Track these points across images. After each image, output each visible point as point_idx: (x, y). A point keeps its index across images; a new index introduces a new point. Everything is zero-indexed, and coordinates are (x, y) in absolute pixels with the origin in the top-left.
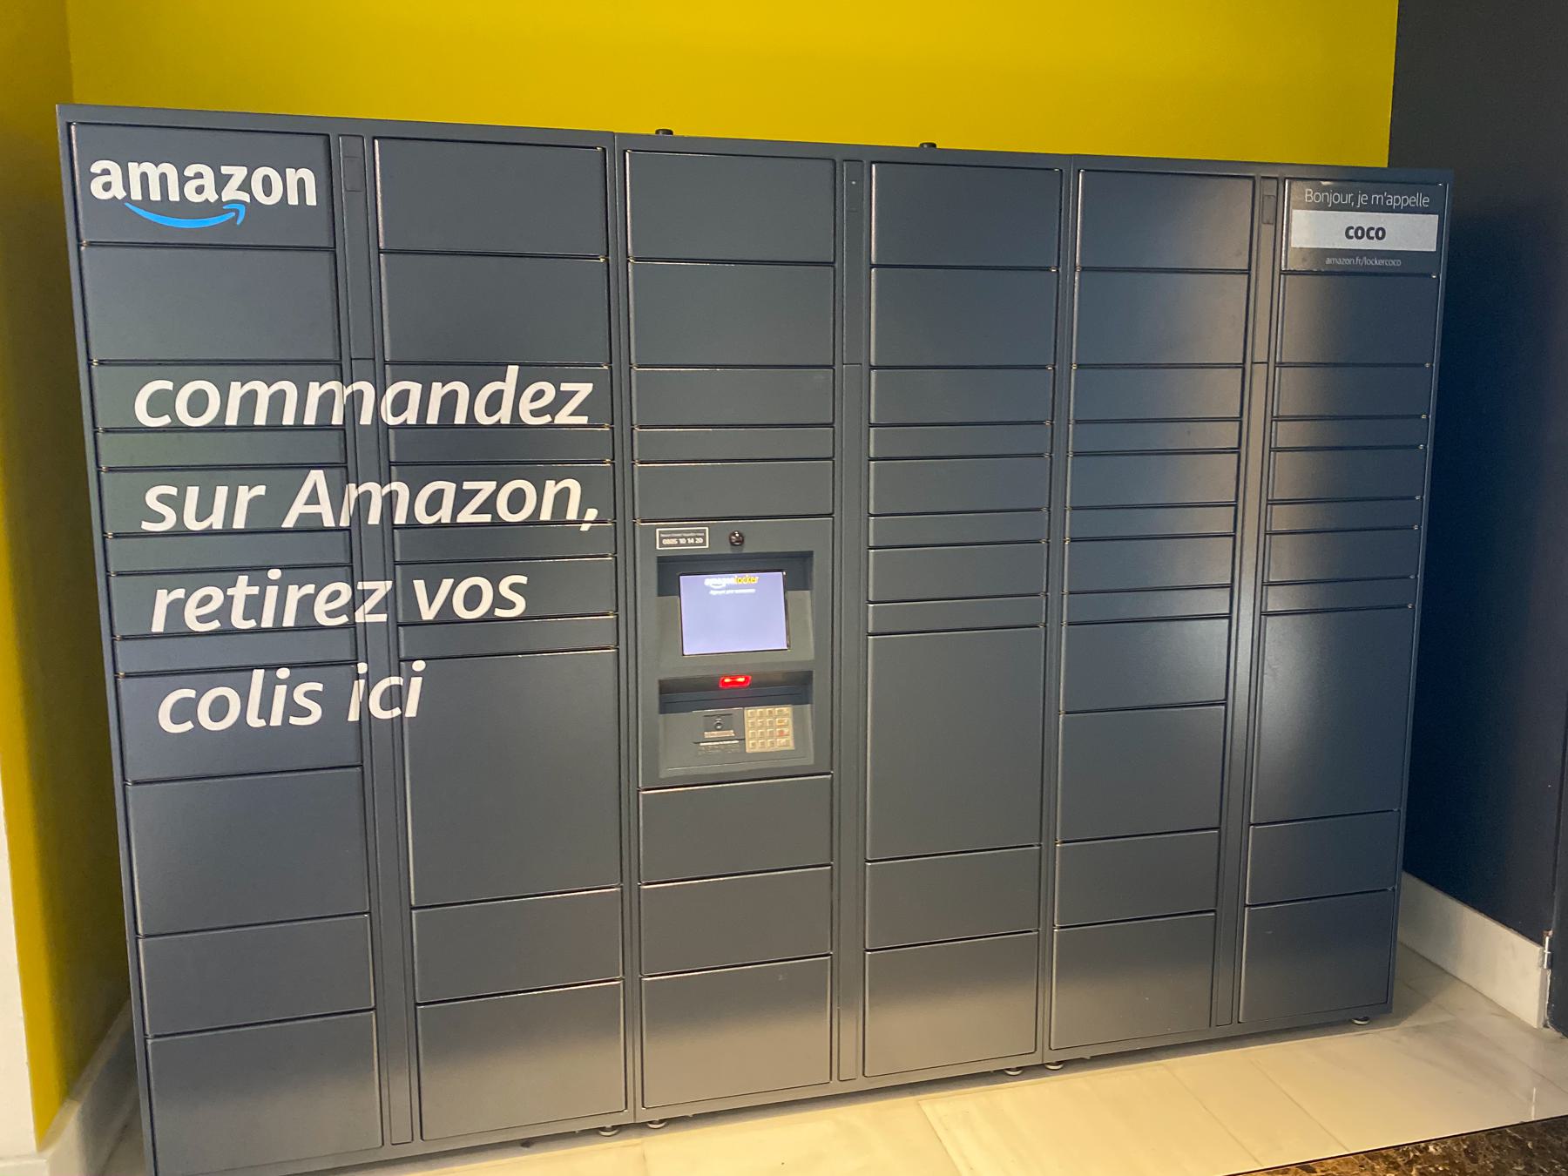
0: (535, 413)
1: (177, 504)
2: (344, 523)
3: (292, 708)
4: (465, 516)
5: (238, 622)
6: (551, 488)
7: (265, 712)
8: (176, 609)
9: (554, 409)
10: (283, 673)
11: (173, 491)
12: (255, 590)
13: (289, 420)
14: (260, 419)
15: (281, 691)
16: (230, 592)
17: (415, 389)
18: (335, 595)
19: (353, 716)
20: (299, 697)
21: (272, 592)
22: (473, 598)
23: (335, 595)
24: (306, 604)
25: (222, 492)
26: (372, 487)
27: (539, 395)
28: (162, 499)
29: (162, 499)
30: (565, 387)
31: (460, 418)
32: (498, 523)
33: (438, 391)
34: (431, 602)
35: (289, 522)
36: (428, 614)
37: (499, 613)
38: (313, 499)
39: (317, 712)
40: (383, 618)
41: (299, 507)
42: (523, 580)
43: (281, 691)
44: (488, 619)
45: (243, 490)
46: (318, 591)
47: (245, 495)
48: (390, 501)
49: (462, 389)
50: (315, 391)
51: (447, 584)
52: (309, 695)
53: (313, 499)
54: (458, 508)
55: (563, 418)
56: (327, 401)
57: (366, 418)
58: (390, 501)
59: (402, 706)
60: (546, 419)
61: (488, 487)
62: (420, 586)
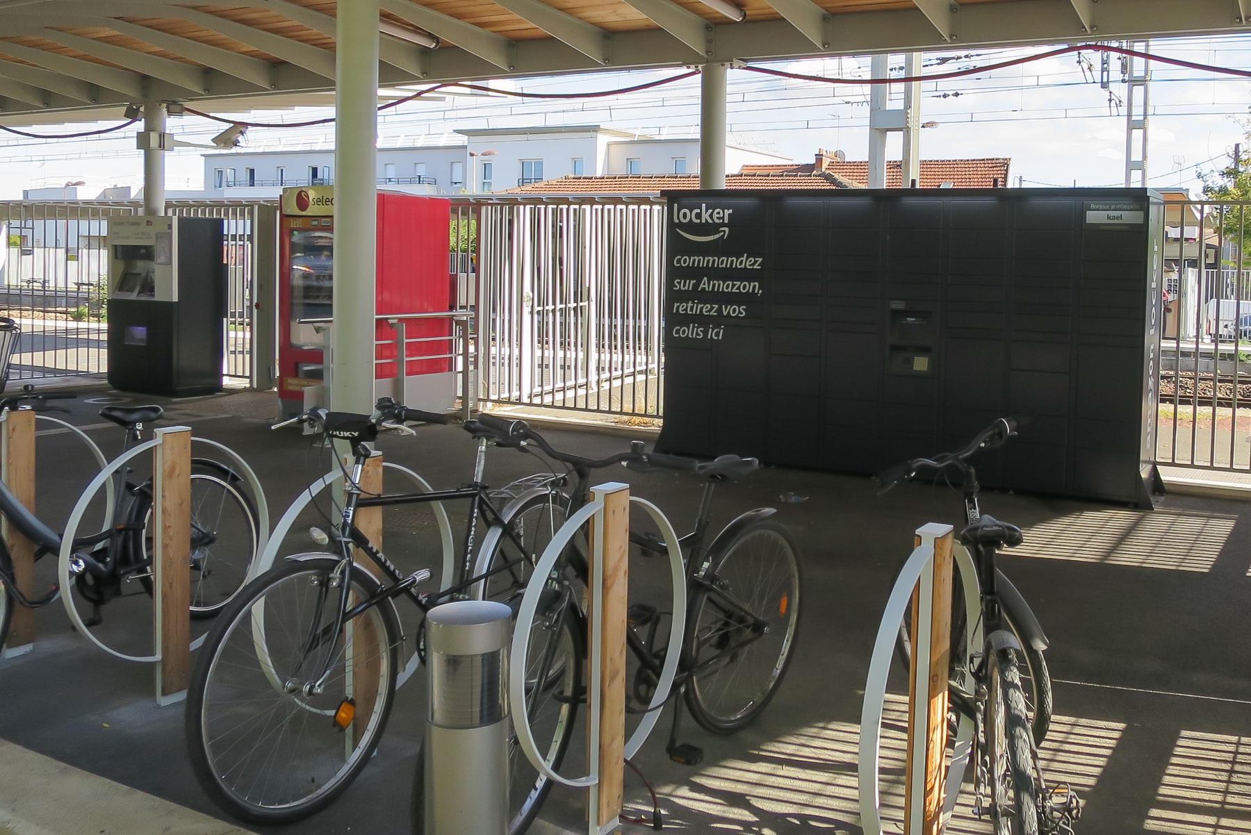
1: (680, 283)
2: (710, 290)
3: (697, 334)
5: (689, 312)
6: (752, 284)
7: (692, 335)
8: (678, 307)
9: (754, 264)
10: (696, 325)
13: (701, 266)
15: (695, 329)
17: (725, 259)
18: (707, 307)
20: (699, 332)
21: (695, 305)
22: (734, 311)
23: (707, 307)
24: (702, 308)
27: (751, 261)
28: (677, 282)
29: (677, 282)
36: (725, 314)
38: (704, 284)
41: (702, 286)
43: (695, 329)
44: (737, 316)
47: (692, 282)
50: (706, 259)
52: (701, 331)
54: (732, 288)
55: (755, 267)
56: (709, 261)
61: (739, 283)
62: (724, 306)
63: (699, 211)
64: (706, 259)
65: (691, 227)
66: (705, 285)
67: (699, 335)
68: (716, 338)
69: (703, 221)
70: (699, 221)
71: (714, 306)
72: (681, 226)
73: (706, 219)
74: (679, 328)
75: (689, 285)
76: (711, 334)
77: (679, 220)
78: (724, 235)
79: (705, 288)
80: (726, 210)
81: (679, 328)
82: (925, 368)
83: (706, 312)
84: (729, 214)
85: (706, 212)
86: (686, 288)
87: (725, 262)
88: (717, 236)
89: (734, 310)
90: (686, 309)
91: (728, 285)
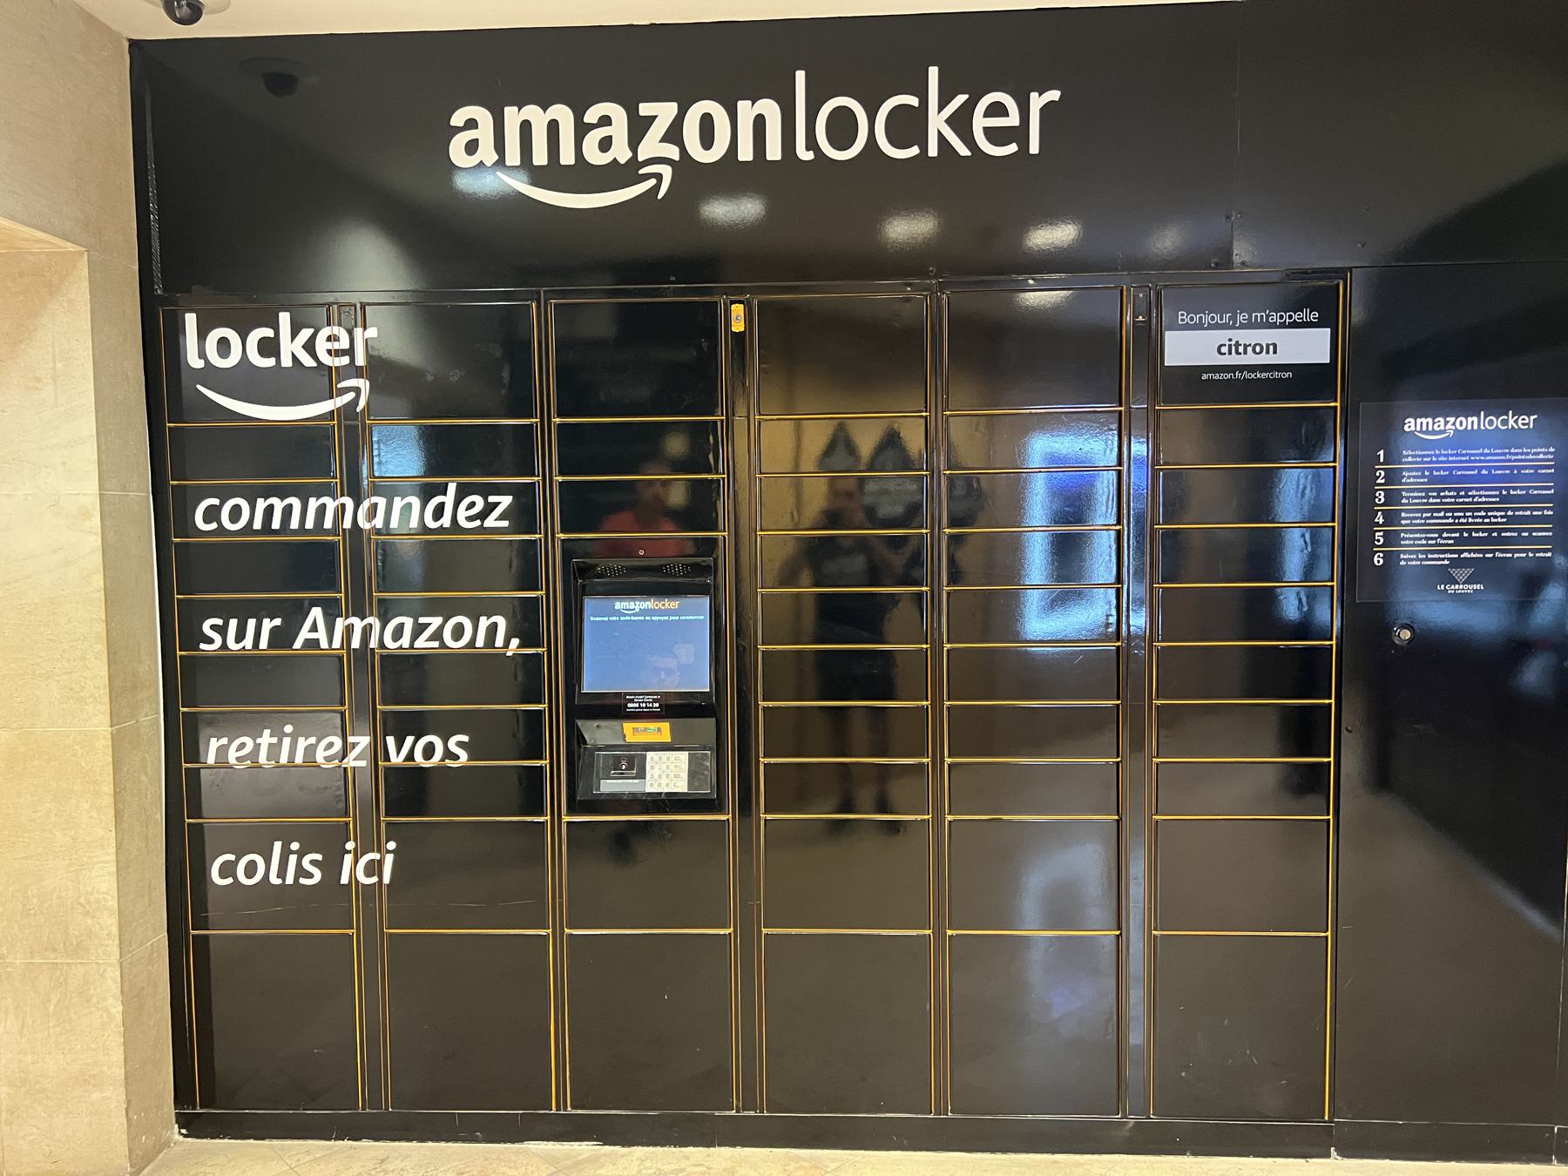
3: (301, 872)
7: (282, 873)
12: (275, 740)
16: (259, 740)
21: (287, 741)
22: (429, 751)
26: (354, 620)
27: (472, 505)
39: (318, 875)
46: (318, 742)
67: (310, 875)
81: (232, 857)
91: (401, 627)
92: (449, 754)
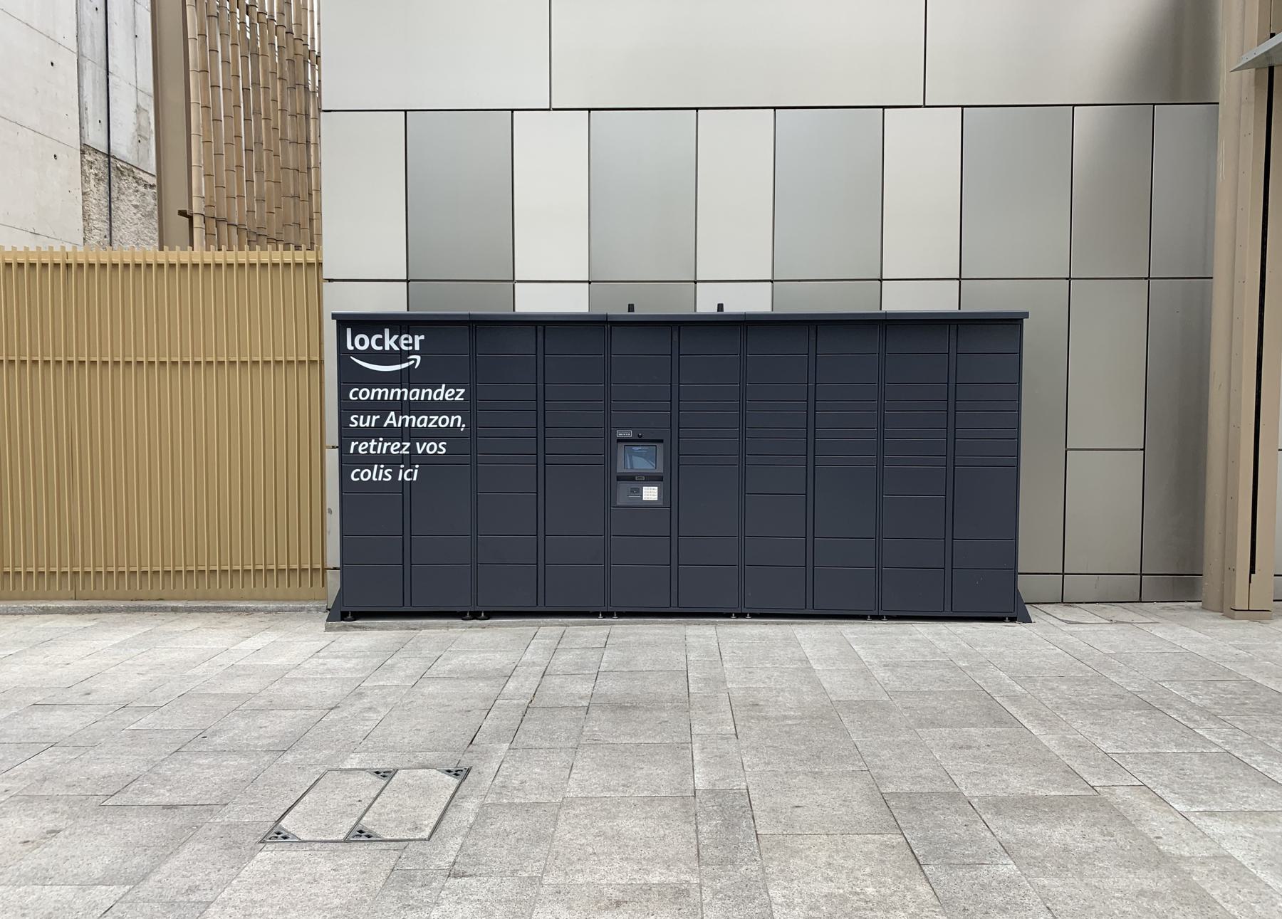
0: (449, 397)
1: (358, 420)
2: (399, 425)
3: (384, 476)
4: (430, 425)
5: (372, 452)
7: (377, 477)
8: (356, 447)
9: (454, 396)
10: (382, 466)
11: (357, 416)
12: (376, 443)
13: (386, 398)
14: (379, 398)
15: (381, 471)
17: (418, 391)
18: (396, 446)
19: (400, 479)
20: (386, 473)
21: (380, 444)
23: (396, 446)
24: (389, 447)
25: (369, 417)
27: (450, 392)
28: (355, 419)
29: (355, 419)
30: (457, 390)
31: (430, 398)
32: (439, 427)
33: (424, 391)
34: (421, 448)
35: (385, 425)
36: (420, 452)
37: (439, 453)
38: (391, 419)
40: (408, 453)
41: (388, 421)
42: (445, 443)
43: (381, 471)
44: (436, 453)
45: (374, 417)
48: (411, 421)
49: (430, 391)
50: (393, 391)
51: (425, 444)
52: (389, 472)
53: (391, 419)
55: (457, 398)
56: (396, 393)
57: (405, 398)
58: (411, 421)
59: (413, 478)
60: (452, 399)
61: (436, 418)
62: (418, 444)
63: (381, 336)
64: (393, 391)
65: (370, 355)
66: (392, 419)
67: (387, 477)
68: (409, 480)
69: (387, 348)
70: (381, 348)
71: (404, 443)
72: (356, 353)
73: (390, 346)
74: (359, 470)
75: (372, 421)
76: (403, 475)
77: (355, 347)
78: (415, 364)
79: (392, 424)
80: (416, 337)
82: (655, 498)
83: (395, 451)
84: (420, 341)
85: (390, 339)
86: (367, 425)
87: (417, 394)
88: (405, 365)
89: (432, 446)
90: (368, 449)
91: (423, 419)
92: (439, 449)
